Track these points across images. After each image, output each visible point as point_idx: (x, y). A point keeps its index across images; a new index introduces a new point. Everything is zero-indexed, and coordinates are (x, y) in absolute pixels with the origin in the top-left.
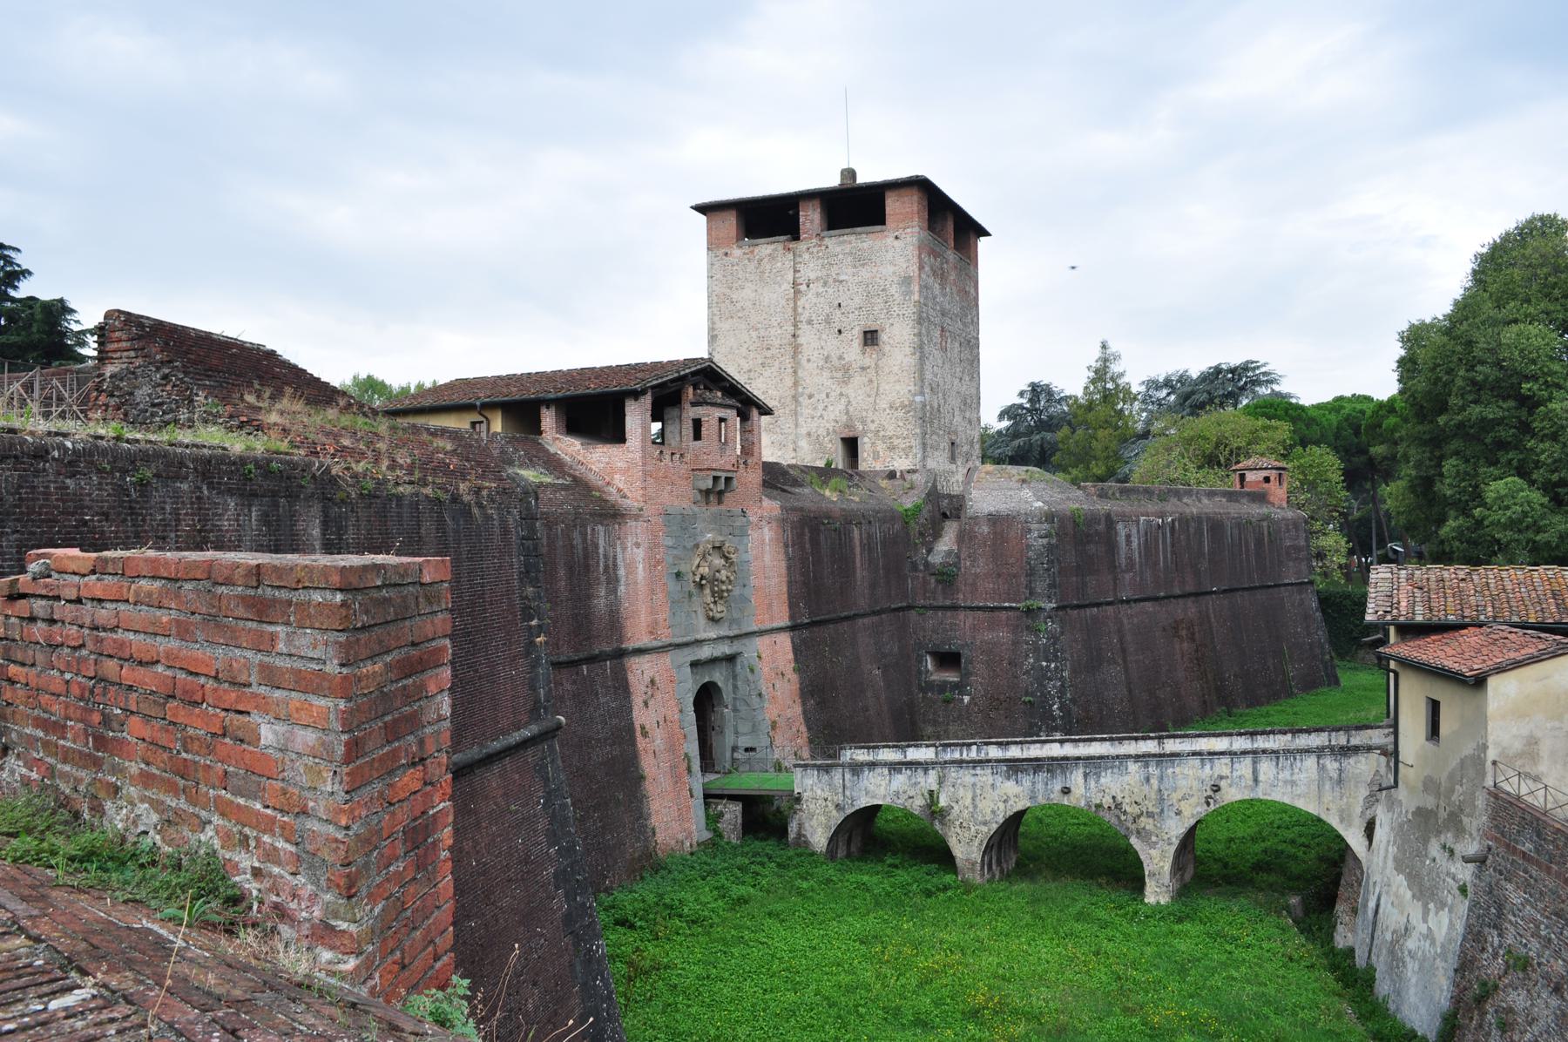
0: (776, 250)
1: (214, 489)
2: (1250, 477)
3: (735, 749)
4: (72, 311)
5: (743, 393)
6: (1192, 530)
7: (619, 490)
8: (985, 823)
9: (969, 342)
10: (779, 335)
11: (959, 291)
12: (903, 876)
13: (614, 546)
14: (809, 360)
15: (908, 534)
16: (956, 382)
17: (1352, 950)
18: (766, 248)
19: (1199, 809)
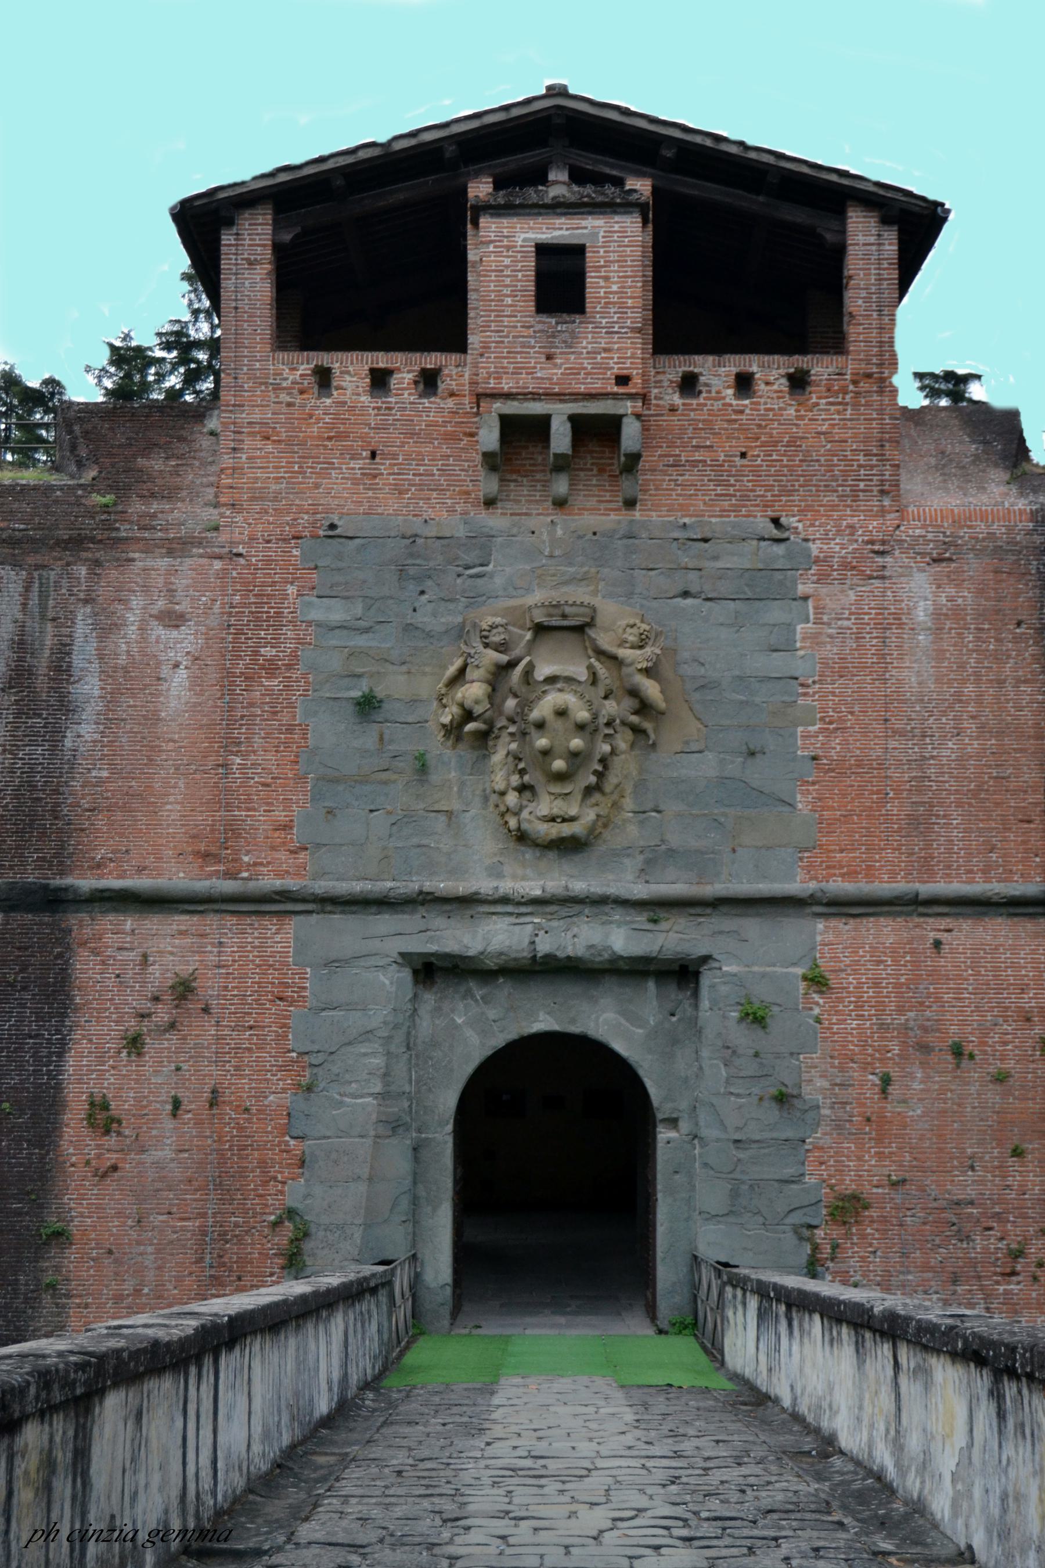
13: (64, 621)
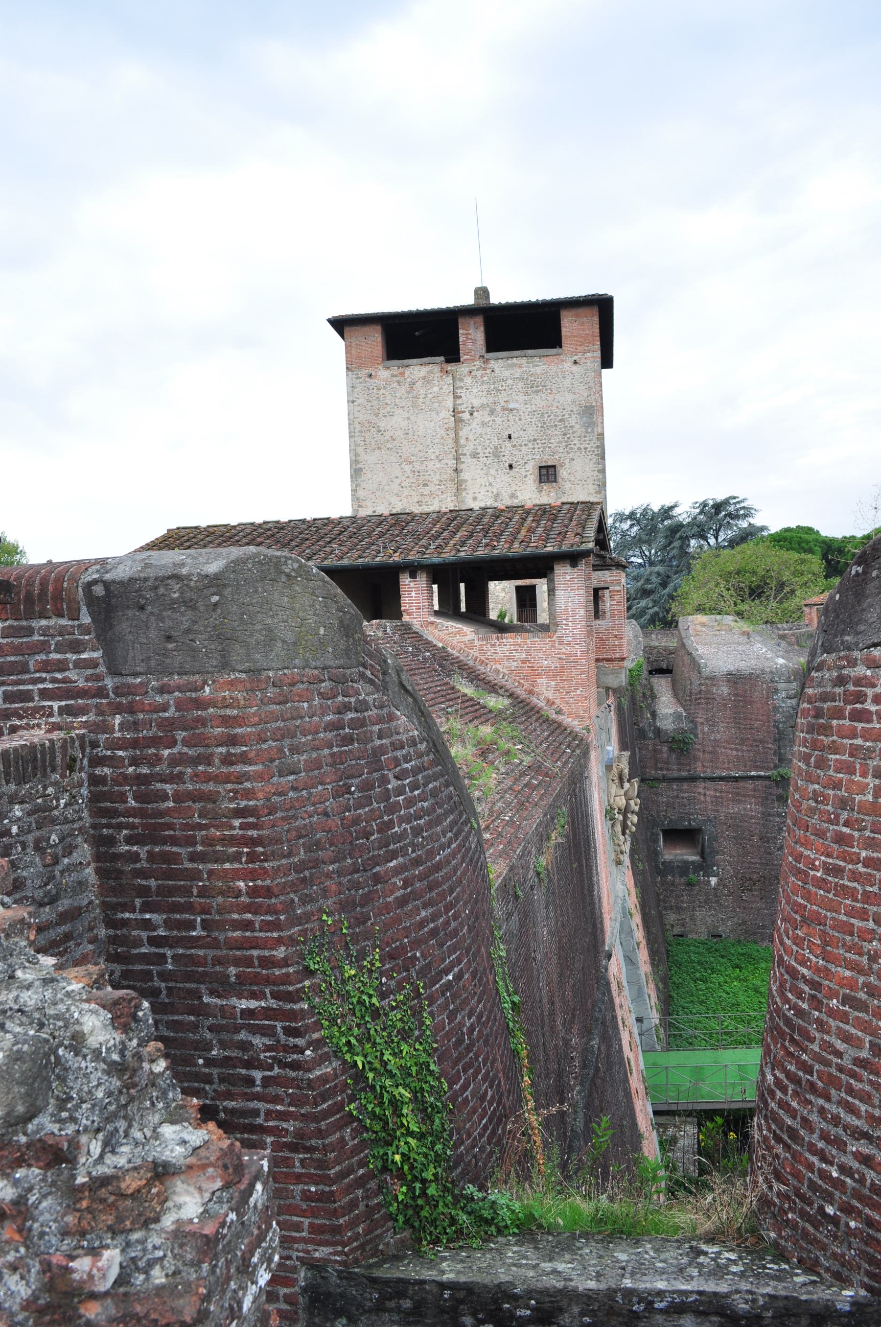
0: (431, 372)
7: (548, 701)
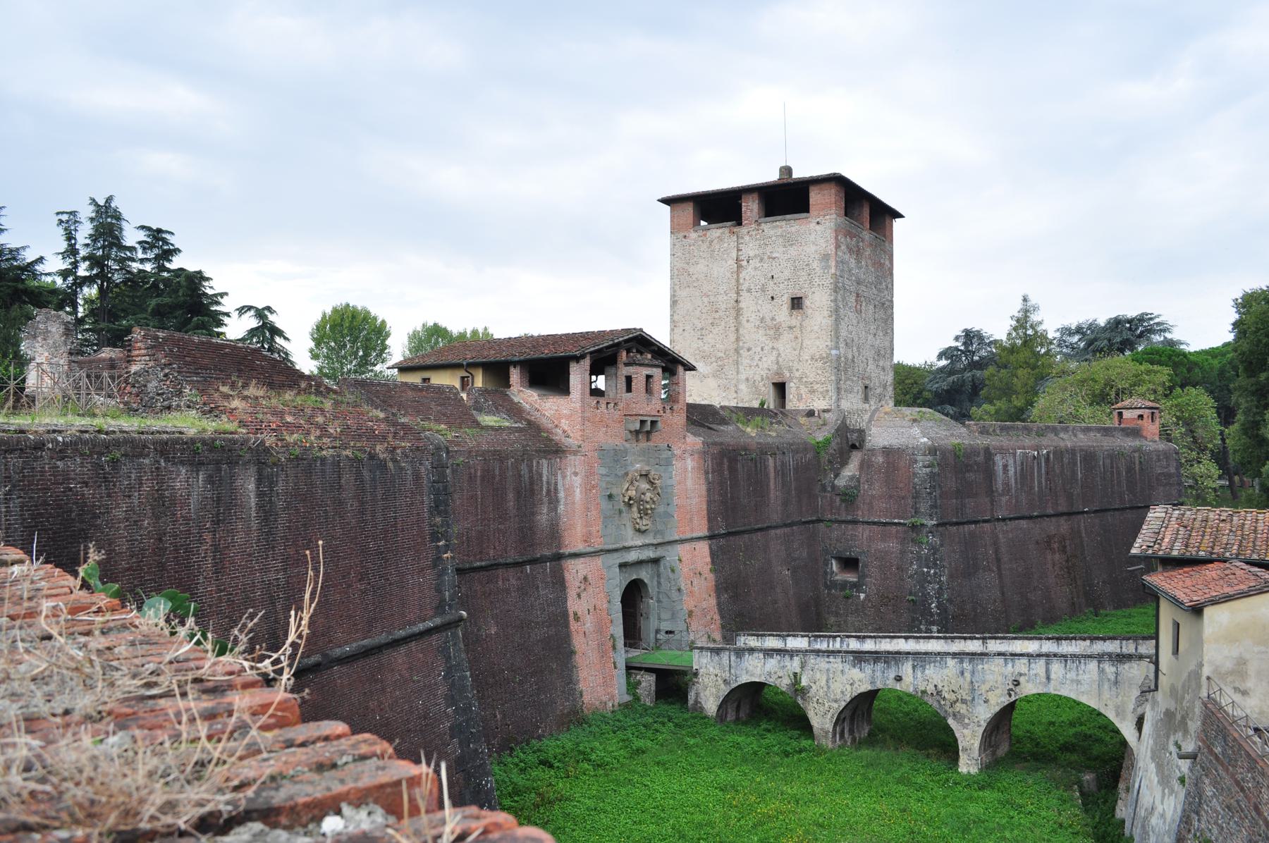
0: (723, 233)
1: (169, 461)
2: (1127, 414)
3: (658, 631)
4: (208, 279)
5: (669, 354)
6: (1066, 460)
7: (564, 432)
8: (836, 701)
9: (883, 304)
10: (725, 301)
11: (874, 264)
12: (771, 739)
13: (556, 475)
14: (748, 321)
15: (819, 462)
16: (870, 337)
17: (1123, 821)
18: (718, 232)
19: (1003, 699)
